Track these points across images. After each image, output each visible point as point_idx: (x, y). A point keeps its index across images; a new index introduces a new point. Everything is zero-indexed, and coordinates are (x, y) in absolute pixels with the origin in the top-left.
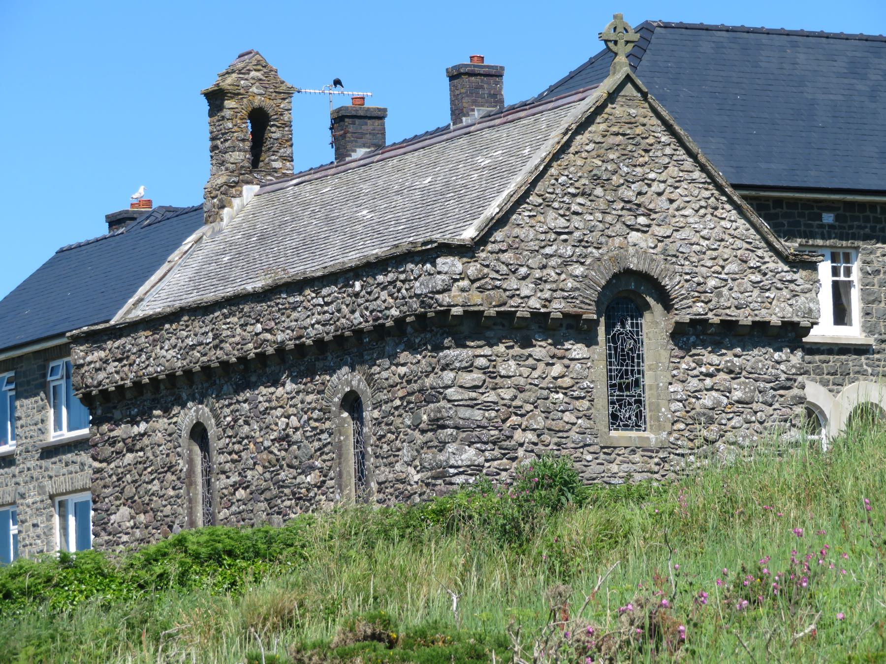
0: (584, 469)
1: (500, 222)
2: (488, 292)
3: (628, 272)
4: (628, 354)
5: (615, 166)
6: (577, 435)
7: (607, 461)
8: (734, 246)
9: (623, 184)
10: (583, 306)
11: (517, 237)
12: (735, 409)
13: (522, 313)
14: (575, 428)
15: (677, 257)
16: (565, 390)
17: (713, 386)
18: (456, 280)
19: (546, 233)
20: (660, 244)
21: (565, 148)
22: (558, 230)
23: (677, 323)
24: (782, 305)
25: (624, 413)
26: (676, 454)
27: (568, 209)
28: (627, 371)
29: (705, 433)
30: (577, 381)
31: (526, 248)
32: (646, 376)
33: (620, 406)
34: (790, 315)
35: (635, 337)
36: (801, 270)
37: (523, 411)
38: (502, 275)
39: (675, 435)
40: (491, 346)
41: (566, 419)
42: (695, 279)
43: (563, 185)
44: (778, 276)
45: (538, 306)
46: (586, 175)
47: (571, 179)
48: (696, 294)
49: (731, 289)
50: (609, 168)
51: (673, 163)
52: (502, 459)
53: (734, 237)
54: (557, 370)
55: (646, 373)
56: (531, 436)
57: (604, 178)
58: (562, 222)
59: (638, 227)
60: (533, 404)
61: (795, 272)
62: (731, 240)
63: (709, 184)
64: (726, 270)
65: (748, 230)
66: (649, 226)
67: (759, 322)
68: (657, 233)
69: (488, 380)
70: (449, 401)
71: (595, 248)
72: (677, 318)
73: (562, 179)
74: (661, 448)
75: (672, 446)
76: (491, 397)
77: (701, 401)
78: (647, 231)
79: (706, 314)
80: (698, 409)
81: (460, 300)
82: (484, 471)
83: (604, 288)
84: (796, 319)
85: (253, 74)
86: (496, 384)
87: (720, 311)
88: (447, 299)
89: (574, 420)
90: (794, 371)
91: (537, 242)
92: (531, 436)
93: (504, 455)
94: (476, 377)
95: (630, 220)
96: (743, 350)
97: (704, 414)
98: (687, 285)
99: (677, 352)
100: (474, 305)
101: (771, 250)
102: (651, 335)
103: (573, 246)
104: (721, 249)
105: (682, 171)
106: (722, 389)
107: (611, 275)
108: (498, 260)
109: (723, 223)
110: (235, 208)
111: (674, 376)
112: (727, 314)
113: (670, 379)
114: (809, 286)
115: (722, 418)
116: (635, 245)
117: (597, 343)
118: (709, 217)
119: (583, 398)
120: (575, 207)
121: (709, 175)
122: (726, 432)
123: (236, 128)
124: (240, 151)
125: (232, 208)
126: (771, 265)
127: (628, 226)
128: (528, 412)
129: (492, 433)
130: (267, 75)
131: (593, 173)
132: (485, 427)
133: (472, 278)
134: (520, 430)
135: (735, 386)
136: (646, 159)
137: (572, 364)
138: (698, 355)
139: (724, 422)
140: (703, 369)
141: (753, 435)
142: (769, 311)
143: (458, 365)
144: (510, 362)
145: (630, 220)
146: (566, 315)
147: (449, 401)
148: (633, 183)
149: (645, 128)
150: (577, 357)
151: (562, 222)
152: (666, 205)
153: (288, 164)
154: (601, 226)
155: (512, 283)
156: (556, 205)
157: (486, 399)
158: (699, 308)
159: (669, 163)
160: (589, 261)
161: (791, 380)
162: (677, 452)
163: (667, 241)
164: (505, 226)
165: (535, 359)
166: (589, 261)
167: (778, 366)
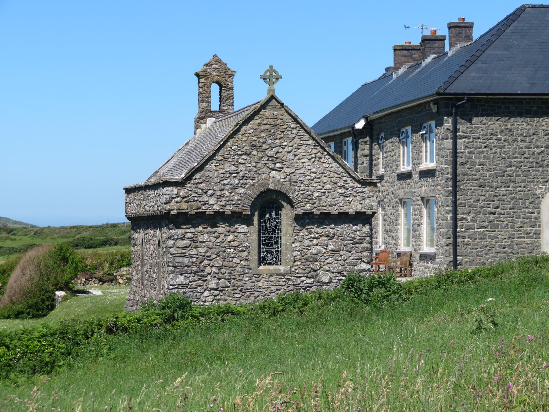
0: (244, 285)
1: (200, 168)
2: (191, 203)
3: (269, 190)
4: (273, 229)
5: (264, 140)
6: (240, 269)
7: (256, 281)
8: (330, 176)
9: (269, 148)
10: (243, 208)
11: (208, 176)
12: (330, 254)
13: (210, 212)
14: (239, 265)
15: (297, 183)
16: (235, 248)
17: (317, 244)
18: (174, 198)
19: (224, 173)
20: (288, 177)
21: (235, 133)
22: (231, 172)
24: (356, 204)
25: (269, 257)
26: (294, 277)
27: (237, 162)
28: (271, 237)
29: (312, 266)
30: (241, 243)
32: (282, 239)
33: (267, 253)
34: (360, 209)
35: (277, 220)
37: (211, 258)
38: (199, 194)
39: (295, 267)
40: (195, 227)
41: (234, 261)
42: (307, 193)
43: (235, 150)
45: (218, 209)
46: (248, 145)
47: (239, 147)
48: (307, 200)
49: (327, 197)
50: (261, 141)
51: (298, 137)
52: (198, 281)
53: (330, 171)
54: (231, 238)
55: (282, 238)
56: (214, 270)
58: (233, 168)
59: (277, 169)
60: (216, 254)
61: (364, 188)
62: (328, 173)
63: (317, 146)
64: (324, 188)
65: (338, 168)
66: (282, 168)
67: (342, 212)
68: (286, 171)
69: (193, 244)
70: (171, 254)
72: (296, 212)
73: (234, 148)
74: (286, 274)
75: (293, 273)
76: (194, 251)
77: (310, 251)
79: (312, 209)
80: (309, 255)
81: (175, 207)
82: (189, 287)
83: (255, 199)
84: (363, 210)
85: (214, 66)
86: (197, 246)
87: (320, 208)
88: (168, 207)
89: (238, 261)
90: (364, 235)
92: (214, 270)
93: (200, 279)
94: (186, 242)
95: (271, 165)
96: (335, 226)
97: (311, 257)
98: (302, 196)
99: (298, 227)
101: (351, 177)
102: (285, 220)
103: (239, 179)
104: (322, 178)
105: (302, 141)
106: (322, 245)
107: (259, 193)
108: (197, 187)
109: (324, 165)
110: (203, 129)
111: (296, 239)
112: (324, 209)
113: (293, 241)
114: (372, 194)
115: (322, 259)
116: (274, 178)
117: (253, 225)
118: (316, 162)
119: (245, 251)
120: (240, 161)
121: (317, 142)
122: (324, 265)
123: (204, 92)
124: (206, 102)
125: (201, 129)
126: (351, 185)
127: (270, 169)
128: (214, 259)
129: (193, 269)
130: (221, 66)
131: (252, 144)
132: (190, 266)
133: (182, 197)
134: (209, 267)
135: (330, 243)
136: (282, 136)
137: (239, 235)
139: (322, 260)
140: (312, 235)
141: (339, 267)
143: (176, 237)
144: (205, 235)
145: (271, 165)
146: (233, 213)
147: (171, 254)
149: (283, 121)
151: (233, 168)
152: (292, 157)
153: (230, 107)
154: (255, 169)
155: (205, 198)
156: (230, 160)
157: (191, 253)
158: (308, 207)
159: (295, 137)
160: (247, 186)
161: (362, 239)
162: (296, 276)
163: (292, 175)
165: (219, 233)
166: (247, 186)
167: (355, 233)
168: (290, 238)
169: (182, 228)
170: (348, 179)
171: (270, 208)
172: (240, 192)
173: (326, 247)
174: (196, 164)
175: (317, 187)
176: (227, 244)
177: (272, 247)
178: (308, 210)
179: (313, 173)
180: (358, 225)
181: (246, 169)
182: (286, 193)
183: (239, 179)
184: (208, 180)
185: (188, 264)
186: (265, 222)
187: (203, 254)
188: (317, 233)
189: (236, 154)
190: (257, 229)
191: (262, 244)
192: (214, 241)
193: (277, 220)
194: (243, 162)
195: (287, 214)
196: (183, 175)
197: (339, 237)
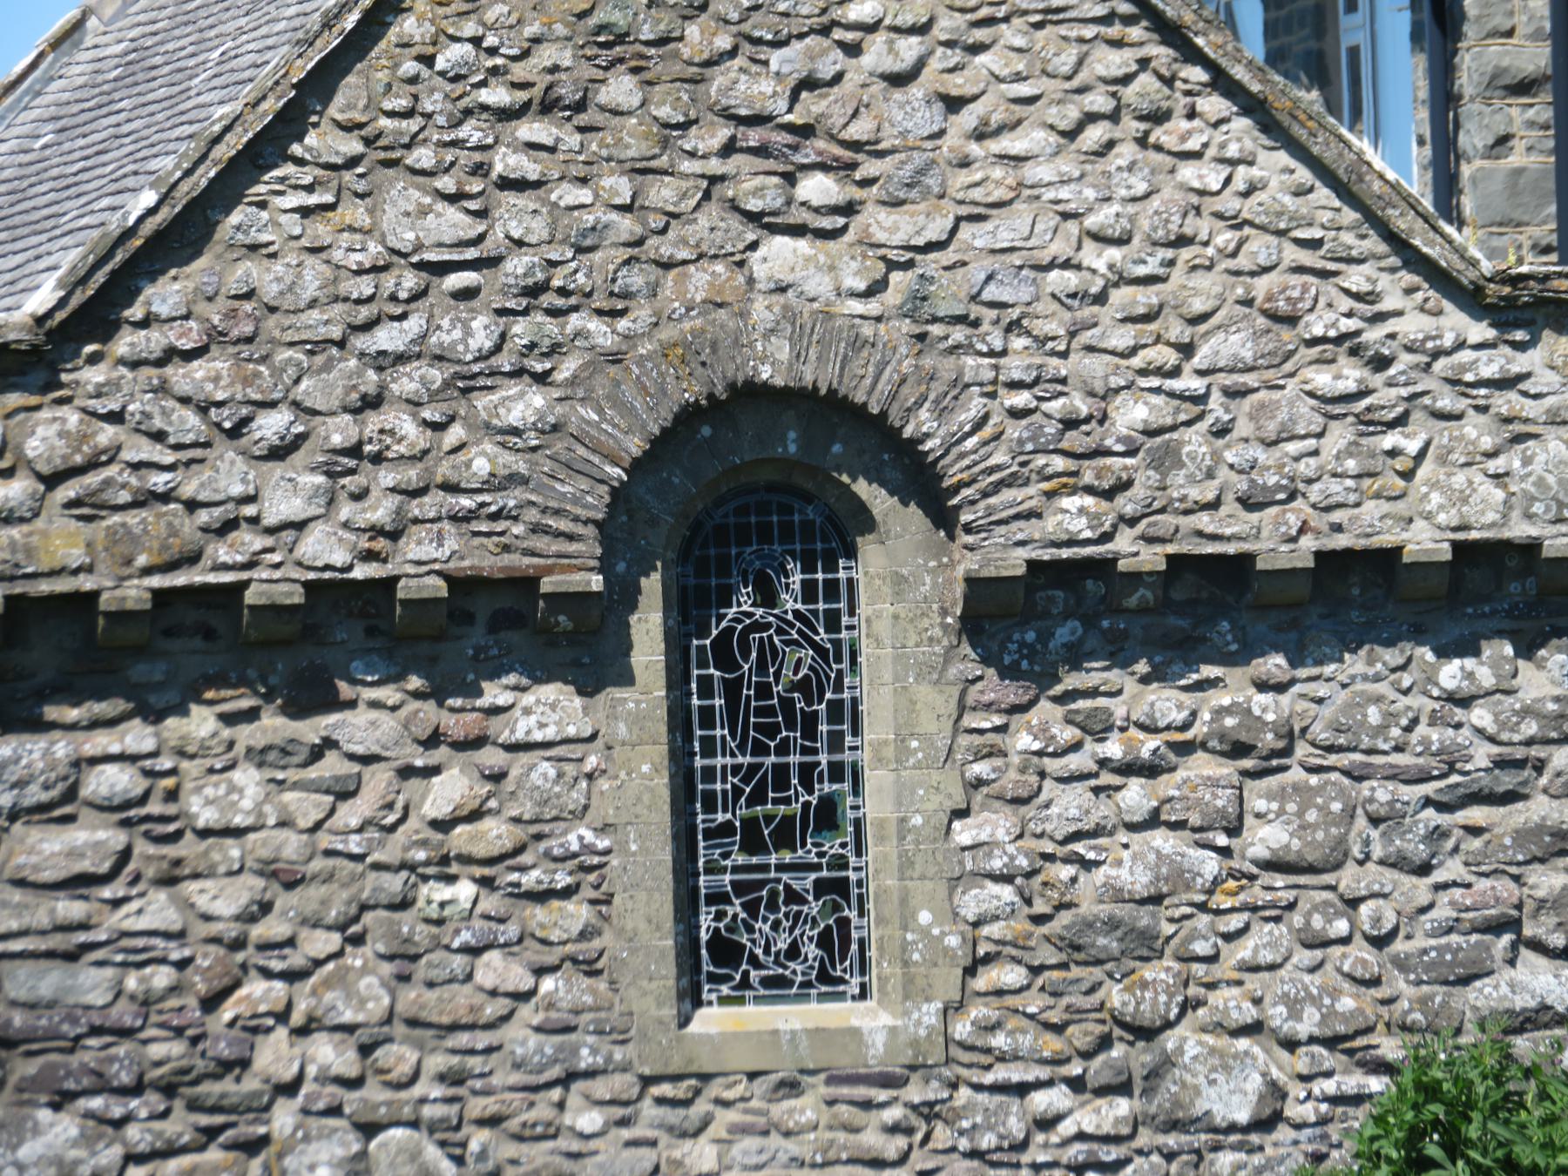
2: (116, 518)
3: (751, 393)
4: (787, 704)
6: (534, 1040)
7: (670, 1129)
8: (1242, 262)
9: (733, 53)
10: (540, 543)
11: (249, 295)
12: (1257, 895)
14: (526, 1012)
15: (976, 324)
17: (1156, 812)
19: (375, 269)
20: (896, 277)
23: (971, 582)
24: (1459, 479)
26: (978, 1088)
27: (480, 170)
28: (781, 772)
29: (1116, 996)
30: (535, 830)
31: (290, 336)
33: (752, 908)
34: (1491, 516)
35: (822, 636)
36: (1548, 336)
37: (296, 960)
38: (178, 447)
40: (154, 716)
42: (1054, 406)
43: (457, 78)
44: (1440, 365)
45: (339, 558)
46: (560, 29)
47: (493, 51)
48: (1059, 463)
49: (1221, 431)
52: (202, 1148)
56: (327, 1053)
57: (647, 33)
58: (452, 222)
59: (805, 217)
60: (341, 927)
61: (1520, 346)
62: (1225, 238)
63: (1129, 20)
64: (1199, 360)
65: (1301, 192)
66: (849, 209)
67: (1348, 553)
68: (880, 236)
69: (142, 848)
71: (600, 312)
72: (970, 564)
73: (450, 56)
74: (913, 1068)
76: (157, 910)
77: (1100, 875)
78: (845, 228)
79: (1106, 537)
80: (1087, 908)
83: (636, 467)
84: (1520, 530)
86: (178, 863)
87: (1168, 521)
89: (520, 978)
90: (1531, 728)
91: (339, 308)
92: (327, 1053)
93: (211, 1133)
95: (758, 192)
97: (1112, 924)
98: (1015, 430)
99: (993, 688)
100: (53, 573)
102: (883, 627)
103: (501, 312)
104: (1177, 275)
106: (1195, 819)
107: (666, 415)
108: (162, 389)
109: (1189, 173)
111: (979, 783)
112: (1200, 534)
115: (1194, 936)
116: (782, 290)
118: (1126, 152)
119: (567, 893)
120: (506, 162)
122: (1212, 986)
126: (1412, 326)
127: (753, 218)
128: (319, 963)
131: (593, 21)
132: (125, 1033)
133: (45, 469)
134: (282, 1033)
135: (1261, 805)
138: (1094, 693)
139: (1201, 948)
140: (1113, 749)
141: (1335, 994)
142: (1400, 507)
144: (237, 776)
146: (462, 585)
148: (778, 44)
150: (538, 736)
151: (452, 222)
152: (929, 118)
154: (626, 226)
156: (423, 157)
160: (567, 368)
161: (1520, 764)
162: (989, 1078)
164: (197, 254)
165: (352, 757)
166: (567, 368)
167: (1459, 714)
168: (936, 776)
169: (53, 726)
170: (1384, 281)
171: (765, 535)
172: (515, 415)
173: (1222, 840)
174: (149, 198)
175: (1133, 351)
176: (423, 843)
177: (788, 857)
178: (1071, 542)
179: (1099, 238)
180: (1476, 652)
181: (553, 226)
182: (884, 414)
183: (501, 312)
184: (248, 329)
185: (114, 1012)
186: (723, 653)
187: (232, 931)
188: (1150, 729)
189: (468, 113)
190: (662, 713)
191: (708, 834)
192: (318, 826)
193: (822, 636)
194: (530, 168)
195: (900, 583)
196: (43, 297)
197: (1331, 749)
